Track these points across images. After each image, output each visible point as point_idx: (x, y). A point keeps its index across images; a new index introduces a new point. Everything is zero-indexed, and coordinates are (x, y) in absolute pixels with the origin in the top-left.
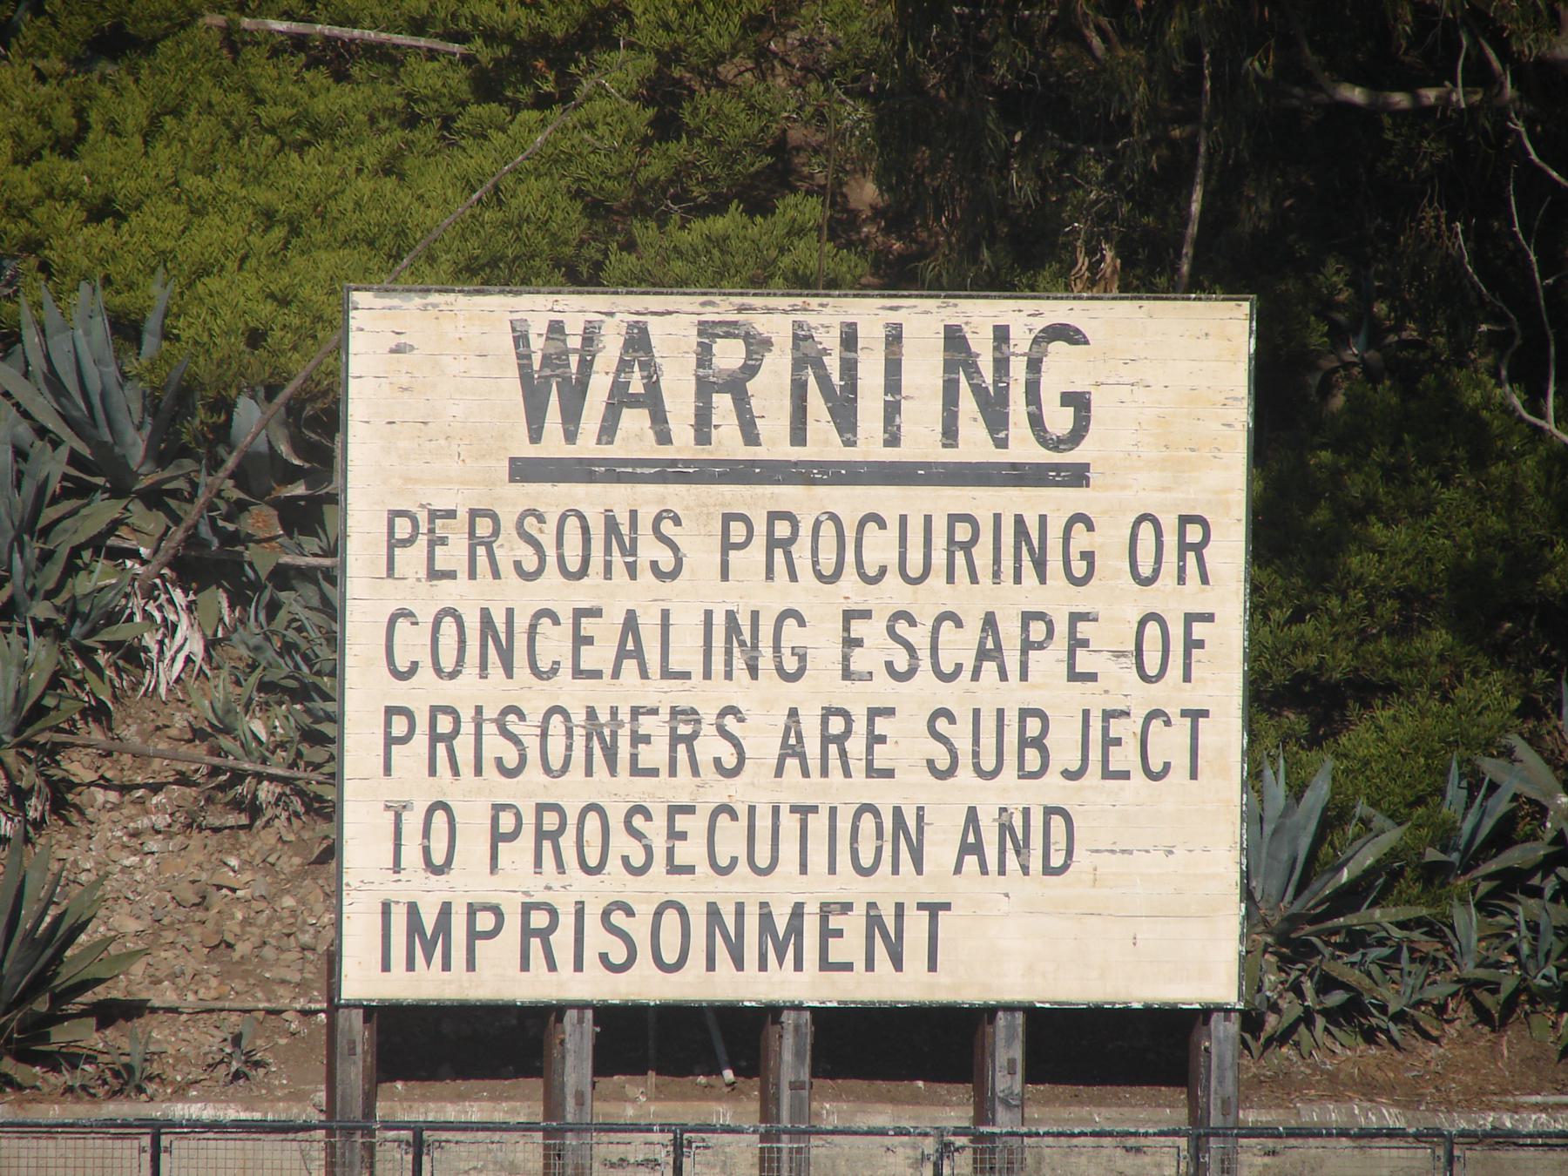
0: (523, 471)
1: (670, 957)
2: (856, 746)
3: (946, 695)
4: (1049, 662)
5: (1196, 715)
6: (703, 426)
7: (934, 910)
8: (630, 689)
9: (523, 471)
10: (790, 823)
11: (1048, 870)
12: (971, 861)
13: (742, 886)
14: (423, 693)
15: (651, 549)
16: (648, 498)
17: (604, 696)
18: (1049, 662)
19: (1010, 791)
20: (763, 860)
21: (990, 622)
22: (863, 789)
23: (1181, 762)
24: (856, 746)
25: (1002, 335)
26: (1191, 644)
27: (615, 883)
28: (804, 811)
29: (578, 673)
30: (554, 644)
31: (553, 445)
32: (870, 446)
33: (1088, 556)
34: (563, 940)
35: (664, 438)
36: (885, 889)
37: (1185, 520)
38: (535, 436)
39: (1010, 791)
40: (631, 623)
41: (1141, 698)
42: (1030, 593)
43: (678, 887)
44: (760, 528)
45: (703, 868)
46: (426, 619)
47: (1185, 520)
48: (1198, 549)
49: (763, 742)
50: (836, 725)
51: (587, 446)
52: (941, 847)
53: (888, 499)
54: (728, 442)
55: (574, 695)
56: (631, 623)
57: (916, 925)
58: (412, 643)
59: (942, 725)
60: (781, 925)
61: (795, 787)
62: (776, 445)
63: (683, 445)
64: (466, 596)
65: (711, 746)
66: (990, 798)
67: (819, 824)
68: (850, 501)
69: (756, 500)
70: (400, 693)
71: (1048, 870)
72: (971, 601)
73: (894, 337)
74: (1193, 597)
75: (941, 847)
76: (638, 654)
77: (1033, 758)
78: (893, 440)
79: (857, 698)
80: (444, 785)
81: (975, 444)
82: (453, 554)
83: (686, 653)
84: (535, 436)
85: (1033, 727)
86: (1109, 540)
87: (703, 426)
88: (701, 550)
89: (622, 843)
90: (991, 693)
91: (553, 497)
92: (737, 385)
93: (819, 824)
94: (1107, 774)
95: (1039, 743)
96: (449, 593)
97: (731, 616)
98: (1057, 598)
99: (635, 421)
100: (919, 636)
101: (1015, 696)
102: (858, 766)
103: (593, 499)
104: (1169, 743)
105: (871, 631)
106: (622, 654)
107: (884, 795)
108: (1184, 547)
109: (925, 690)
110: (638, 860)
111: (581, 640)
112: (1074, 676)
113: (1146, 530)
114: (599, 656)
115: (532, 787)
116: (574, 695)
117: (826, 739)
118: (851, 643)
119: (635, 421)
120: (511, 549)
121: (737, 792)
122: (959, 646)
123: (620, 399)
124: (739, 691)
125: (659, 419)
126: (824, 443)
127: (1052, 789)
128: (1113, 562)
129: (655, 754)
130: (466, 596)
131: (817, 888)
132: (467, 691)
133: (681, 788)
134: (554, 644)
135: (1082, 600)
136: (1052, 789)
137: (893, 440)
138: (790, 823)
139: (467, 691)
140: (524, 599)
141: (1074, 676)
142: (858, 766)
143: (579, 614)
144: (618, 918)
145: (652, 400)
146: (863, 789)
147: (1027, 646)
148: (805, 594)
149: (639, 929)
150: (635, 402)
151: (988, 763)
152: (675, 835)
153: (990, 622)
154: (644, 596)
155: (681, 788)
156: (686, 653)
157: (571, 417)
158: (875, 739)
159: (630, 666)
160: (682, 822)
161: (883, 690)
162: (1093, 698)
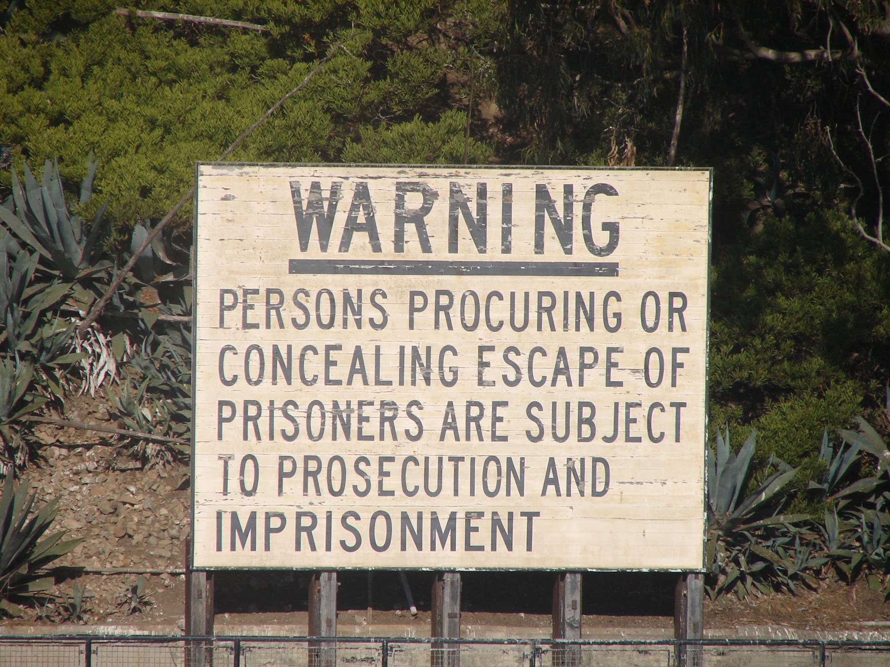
0: (297, 267)
1: (380, 543)
2: (486, 423)
3: (537, 394)
4: (595, 376)
5: (679, 406)
6: (399, 241)
7: (530, 516)
9: (297, 267)
10: (448, 467)
11: (595, 494)
12: (551, 488)
14: (240, 393)
15: (369, 311)
16: (368, 282)
17: (343, 395)
18: (595, 376)
19: (573, 449)
20: (433, 488)
21: (562, 353)
22: (490, 448)
23: (670, 432)
24: (486, 423)
25: (568, 190)
26: (676, 365)
27: (349, 501)
28: (456, 460)
29: (328, 382)
30: (315, 365)
31: (314, 252)
32: (494, 253)
33: (618, 316)
34: (319, 533)
35: (377, 248)
36: (503, 504)
37: (672, 295)
38: (304, 247)
39: (573, 449)
40: (358, 353)
41: (647, 396)
42: (585, 337)
43: (385, 503)
44: (432, 299)
45: (399, 492)
46: (242, 351)
47: (672, 295)
48: (680, 311)
49: (433, 421)
50: (475, 411)
51: (333, 253)
52: (534, 480)
53: (504, 283)
54: (413, 251)
55: (326, 394)
56: (358, 353)
57: (520, 525)
58: (234, 365)
59: (535, 411)
60: (443, 525)
61: (451, 447)
62: (440, 252)
63: (388, 252)
64: (265, 338)
65: (403, 423)
66: (562, 453)
67: (465, 467)
68: (482, 284)
69: (429, 283)
70: (227, 393)
71: (595, 494)
72: (551, 341)
73: (508, 191)
74: (677, 339)
75: (534, 480)
76: (362, 371)
77: (586, 430)
78: (507, 249)
79: (486, 396)
80: (252, 445)
81: (553, 252)
82: (257, 314)
83: (389, 371)
84: (304, 247)
85: (587, 413)
86: (629, 306)
87: (399, 241)
88: (398, 312)
89: (353, 478)
90: (563, 393)
91: (314, 282)
92: (418, 218)
93: (465, 467)
94: (629, 439)
95: (589, 422)
96: (255, 336)
97: (415, 349)
98: (600, 339)
99: (360, 239)
100: (522, 361)
101: (576, 395)
102: (487, 435)
103: (336, 283)
104: (664, 422)
105: (495, 358)
106: (353, 371)
107: (502, 451)
108: (672, 310)
109: (525, 391)
110: (362, 488)
111: (330, 363)
112: (609, 383)
113: (651, 300)
114: (340, 372)
115: (302, 447)
116: (326, 394)
117: (469, 419)
118: (483, 365)
119: (360, 239)
120: (290, 311)
121: (418, 449)
122: (544, 366)
123: (352, 226)
124: (420, 392)
125: (374, 237)
126: (468, 251)
127: (597, 448)
128: (632, 319)
129: (372, 428)
130: (265, 338)
131: (463, 504)
132: (265, 392)
133: (386, 447)
134: (315, 365)
135: (614, 340)
136: (597, 448)
137: (507, 249)
138: (448, 467)
139: (265, 392)
140: (298, 340)
141: (609, 383)
142: (487, 435)
143: (329, 348)
144: (351, 521)
145: (370, 227)
146: (490, 448)
147: (583, 366)
148: (457, 337)
150: (360, 228)
151: (561, 433)
152: (383, 474)
153: (562, 353)
154: (365, 338)
155: (386, 447)
156: (389, 371)
157: (324, 237)
158: (496, 419)
159: (358, 377)
160: (387, 466)
161: (501, 391)
162: (621, 396)
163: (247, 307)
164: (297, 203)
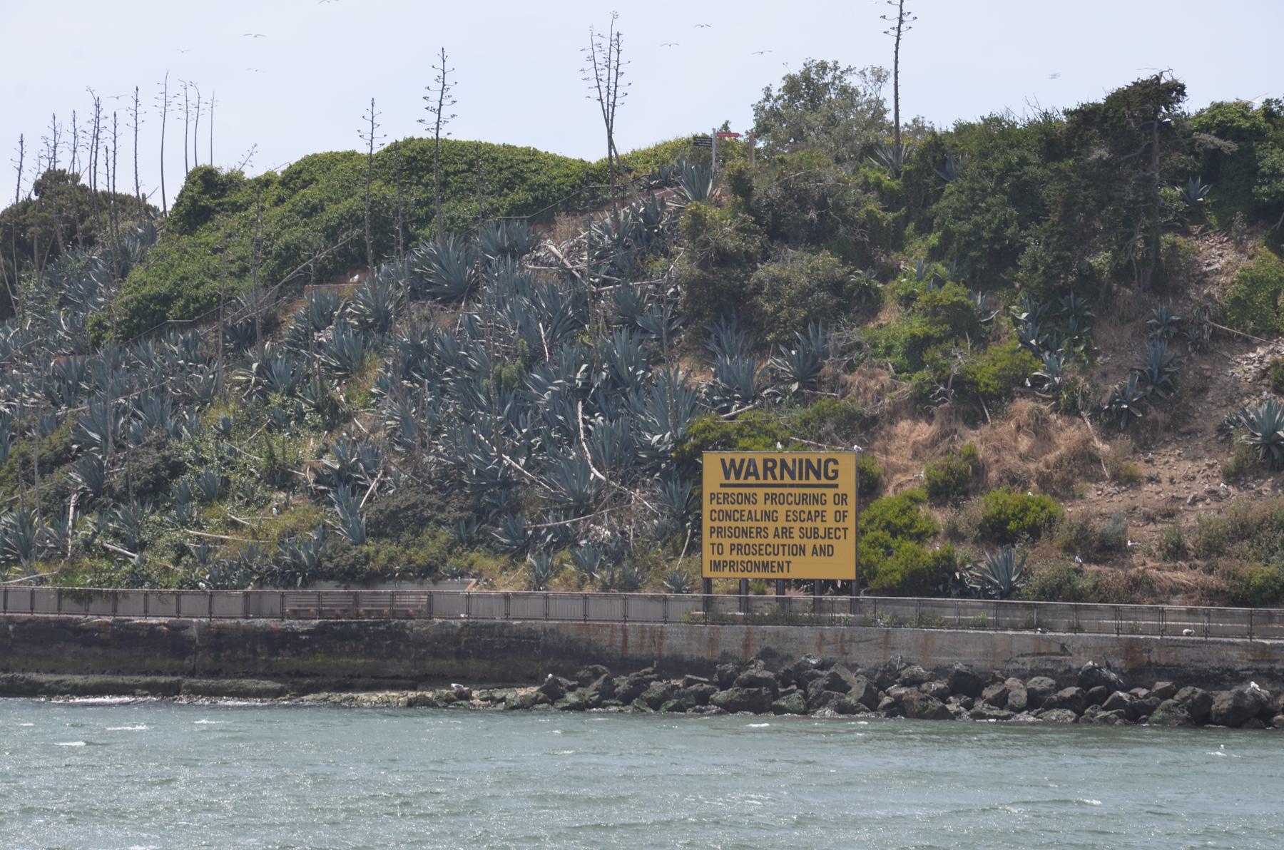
10: (781, 548)
14: (716, 524)
28: (784, 546)
30: (737, 516)
40: (750, 512)
56: (750, 512)
58: (715, 515)
67: (786, 548)
83: (759, 517)
90: (809, 524)
93: (786, 548)
111: (742, 516)
138: (781, 548)
148: (778, 507)
154: (752, 507)
156: (759, 517)
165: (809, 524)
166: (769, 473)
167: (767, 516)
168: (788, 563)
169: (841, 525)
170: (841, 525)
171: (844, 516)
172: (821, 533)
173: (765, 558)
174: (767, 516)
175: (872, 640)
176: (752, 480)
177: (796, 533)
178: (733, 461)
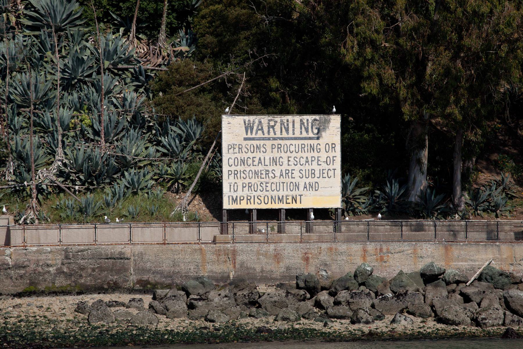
0: (245, 139)
1: (266, 202)
2: (290, 174)
3: (302, 167)
4: (314, 163)
5: (334, 170)
6: (269, 132)
7: (301, 196)
8: (260, 168)
9: (245, 139)
10: (281, 184)
11: (315, 190)
12: (305, 189)
13: (275, 193)
14: (233, 168)
15: (262, 149)
16: (262, 142)
17: (256, 168)
18: (314, 163)
19: (310, 180)
20: (278, 189)
21: (307, 158)
22: (291, 180)
23: (333, 176)
24: (290, 174)
25: (308, 120)
26: (334, 160)
27: (259, 193)
28: (283, 183)
29: (253, 165)
30: (250, 162)
31: (249, 135)
32: (291, 135)
33: (320, 149)
34: (252, 200)
35: (264, 134)
36: (294, 193)
37: (332, 144)
38: (247, 134)
39: (310, 180)
40: (260, 159)
41: (327, 167)
42: (312, 154)
43: (267, 193)
44: (277, 146)
45: (270, 191)
46: (233, 159)
47: (332, 144)
48: (334, 148)
49: (278, 174)
50: (287, 172)
51: (254, 136)
52: (301, 187)
53: (294, 142)
54: (272, 135)
55: (253, 168)
56: (260, 159)
57: (298, 198)
58: (231, 162)
59: (301, 171)
60: (281, 198)
61: (282, 180)
62: (278, 135)
63: (266, 135)
64: (239, 156)
65: (271, 175)
66: (307, 181)
67: (285, 184)
68: (288, 142)
69: (276, 142)
70: (230, 169)
71: (315, 190)
72: (305, 155)
73: (294, 122)
74: (334, 154)
75: (301, 187)
76: (261, 163)
77: (313, 176)
78: (294, 134)
79: (290, 168)
80: (236, 181)
81: (304, 134)
82: (237, 150)
83: (267, 163)
84: (247, 134)
85: (313, 172)
86: (322, 147)
87: (269, 132)
88: (269, 149)
89: (259, 187)
90: (308, 167)
91: (250, 142)
92: (273, 127)
93: (285, 184)
94: (323, 178)
95: (314, 174)
96: (236, 155)
97: (273, 158)
98: (316, 154)
99: (260, 132)
100: (298, 160)
101: (310, 168)
102: (290, 177)
103: (255, 143)
104: (331, 173)
105: (291, 159)
106: (259, 163)
107: (293, 181)
108: (332, 148)
109: (299, 167)
110: (262, 190)
111: (253, 161)
112: (318, 165)
113: (327, 145)
114: (256, 163)
115: (247, 181)
116: (253, 168)
117: (286, 174)
118: (289, 161)
119: (260, 132)
120: (244, 149)
121: (274, 180)
122: (303, 161)
123: (258, 130)
124: (274, 167)
125: (263, 132)
126: (285, 135)
127: (316, 180)
128: (323, 150)
129: (263, 176)
130: (239, 156)
131: (285, 193)
132: (239, 168)
133: (267, 180)
134: (250, 162)
135: (319, 155)
136: (316, 180)
137: (294, 134)
138: (281, 184)
139: (239, 168)
140: (246, 156)
141: (318, 165)
142: (290, 177)
143: (253, 158)
144: (259, 197)
145: (262, 129)
146: (291, 180)
147: (312, 161)
148: (283, 155)
149: (262, 199)
150: (259, 130)
151: (307, 176)
152: (266, 186)
153: (307, 158)
154: (261, 155)
155: (267, 180)
156: (267, 163)
157: (252, 132)
158: (292, 173)
159: (260, 164)
160: (267, 185)
161: (293, 167)
162: (321, 168)
163: (234, 148)
164: (245, 124)
165: (308, 167)
166: (271, 129)
167: (274, 161)
168: (301, 196)
169: (331, 167)
170: (331, 167)
171: (334, 160)
172: (317, 174)
173: (281, 193)
174: (274, 161)
175: (403, 251)
176: (260, 134)
177: (296, 174)
178: (249, 121)
